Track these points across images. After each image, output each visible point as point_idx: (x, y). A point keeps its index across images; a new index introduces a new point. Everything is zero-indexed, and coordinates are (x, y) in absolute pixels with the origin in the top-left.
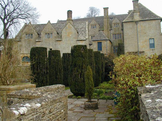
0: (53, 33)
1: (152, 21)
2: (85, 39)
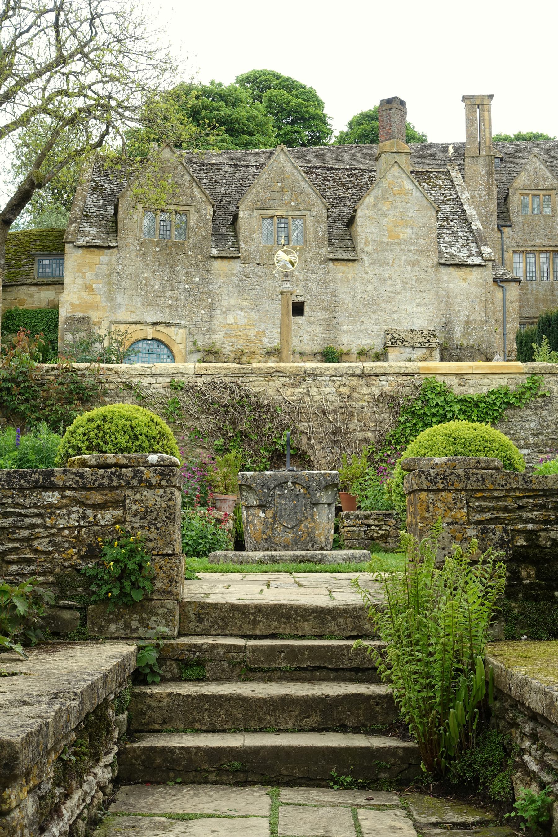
2: (476, 260)
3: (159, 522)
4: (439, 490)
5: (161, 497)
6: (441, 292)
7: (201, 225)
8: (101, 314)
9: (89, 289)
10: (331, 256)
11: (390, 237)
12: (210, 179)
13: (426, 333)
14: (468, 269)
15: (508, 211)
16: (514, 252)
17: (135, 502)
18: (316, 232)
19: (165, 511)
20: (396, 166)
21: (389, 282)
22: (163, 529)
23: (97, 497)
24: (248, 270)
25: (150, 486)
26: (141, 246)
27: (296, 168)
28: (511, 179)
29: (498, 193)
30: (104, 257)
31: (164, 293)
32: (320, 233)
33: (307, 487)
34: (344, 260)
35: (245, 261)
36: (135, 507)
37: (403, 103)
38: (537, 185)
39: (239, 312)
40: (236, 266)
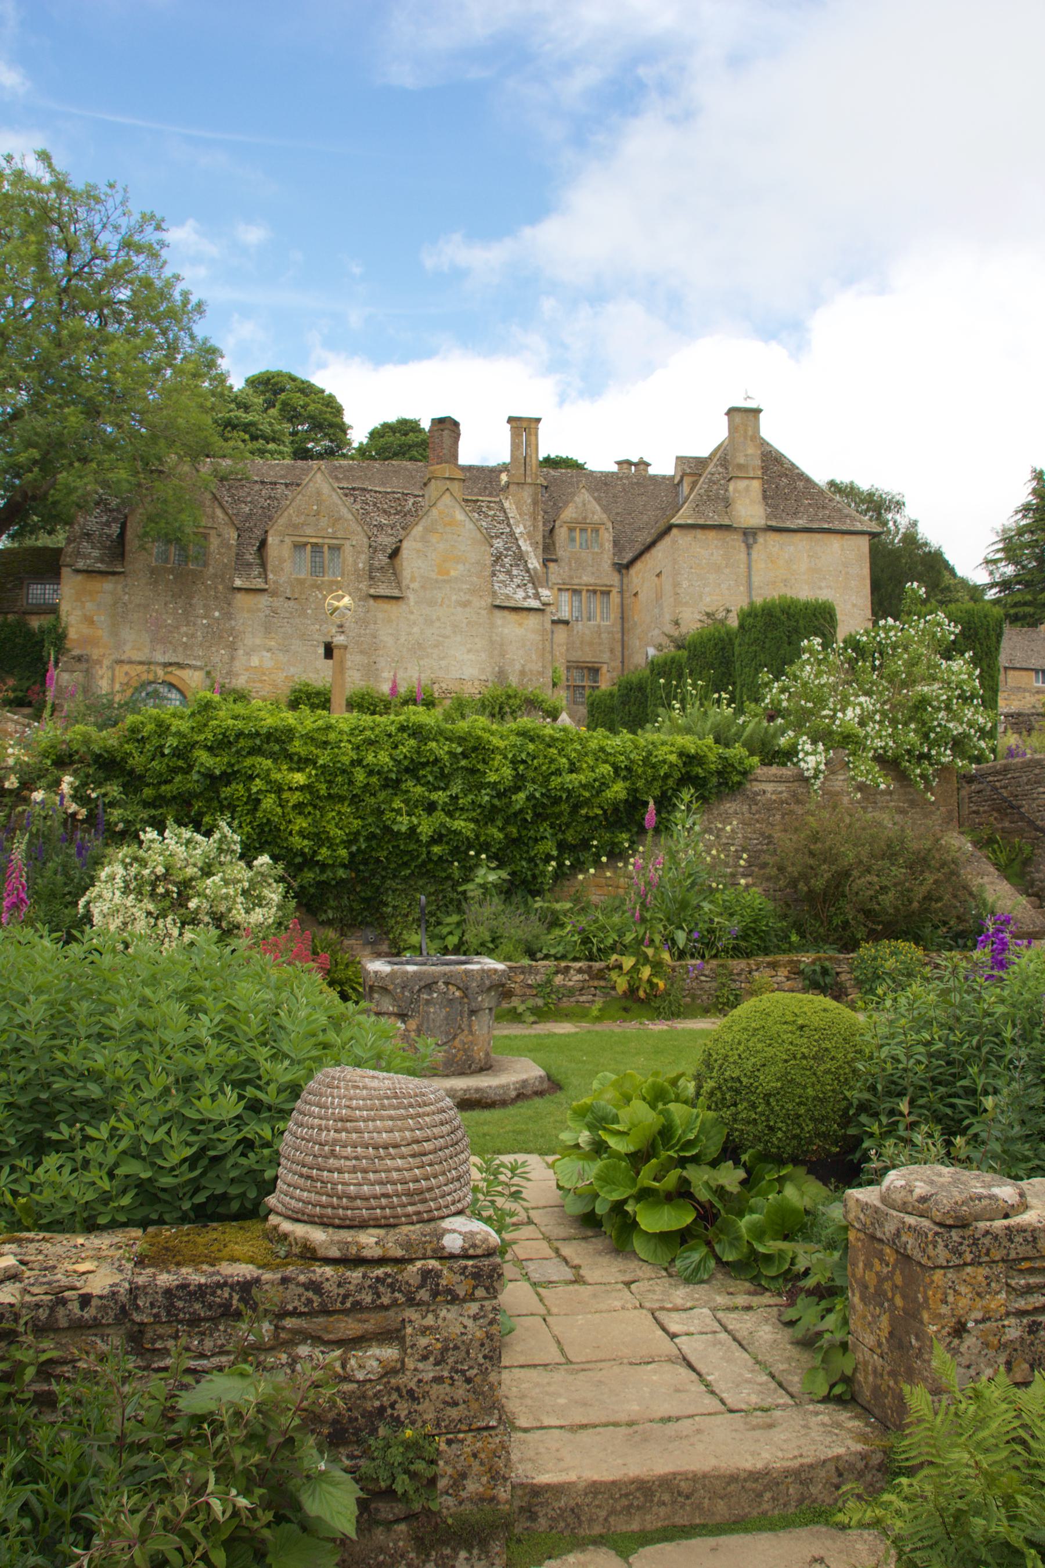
0: (348, 543)
1: (825, 536)
2: (534, 604)
3: (471, 1367)
4: (965, 1264)
5: (475, 1318)
6: (495, 638)
7: (223, 550)
8: (102, 651)
9: (90, 621)
10: (372, 591)
11: (439, 573)
12: (232, 496)
13: (476, 683)
14: (525, 614)
15: (554, 544)
16: (560, 590)
17: (424, 1331)
18: (356, 563)
19: (482, 1345)
20: (448, 494)
21: (437, 624)
22: (478, 1380)
23: (350, 1327)
24: (276, 604)
25: (454, 1299)
26: (152, 573)
27: (334, 490)
28: (558, 509)
29: (544, 524)
30: (108, 585)
31: (177, 628)
32: (361, 565)
33: (465, 990)
34: (387, 597)
35: (274, 594)
36: (423, 1341)
37: (456, 424)
38: (585, 518)
39: (265, 654)
40: (264, 600)
